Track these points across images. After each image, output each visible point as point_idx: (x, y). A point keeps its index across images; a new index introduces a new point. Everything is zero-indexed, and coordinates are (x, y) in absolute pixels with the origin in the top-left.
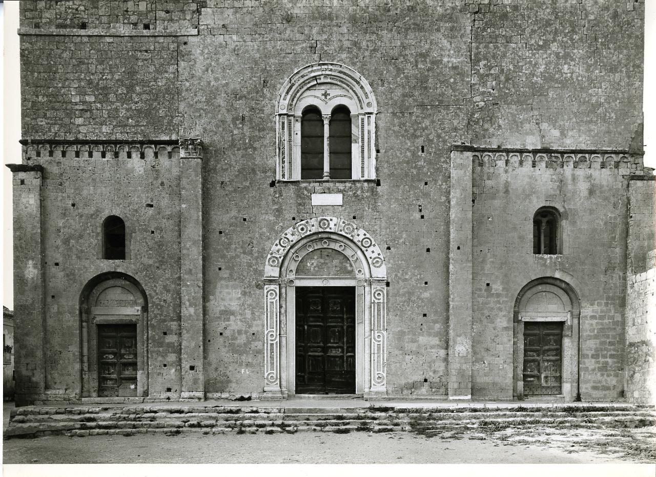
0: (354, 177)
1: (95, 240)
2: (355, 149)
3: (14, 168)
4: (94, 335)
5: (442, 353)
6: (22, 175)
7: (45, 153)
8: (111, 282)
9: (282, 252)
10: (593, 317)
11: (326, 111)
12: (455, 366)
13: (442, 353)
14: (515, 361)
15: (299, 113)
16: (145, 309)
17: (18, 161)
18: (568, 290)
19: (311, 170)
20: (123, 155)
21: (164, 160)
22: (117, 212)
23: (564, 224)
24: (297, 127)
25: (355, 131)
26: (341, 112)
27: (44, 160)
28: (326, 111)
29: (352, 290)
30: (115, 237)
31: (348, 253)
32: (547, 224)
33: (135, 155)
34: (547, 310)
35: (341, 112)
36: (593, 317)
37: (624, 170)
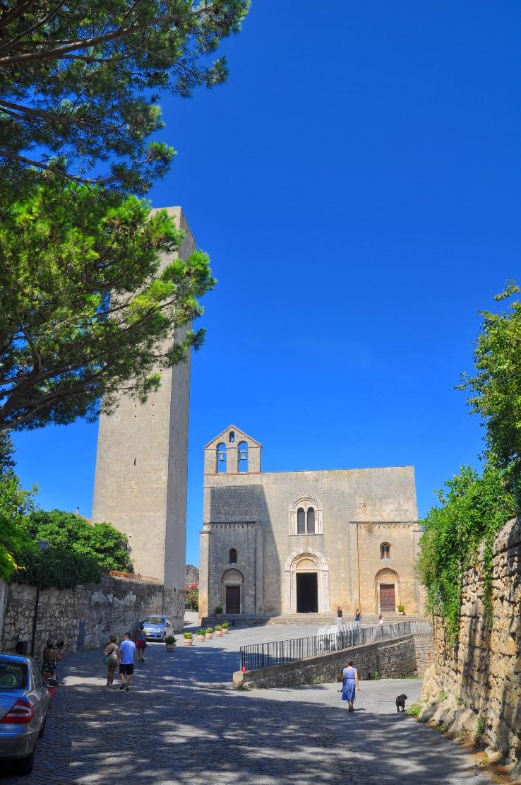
0: (316, 532)
1: (228, 558)
2: (316, 522)
4: (225, 591)
5: (349, 597)
8: (229, 572)
9: (291, 560)
10: (404, 582)
11: (306, 510)
12: (353, 602)
13: (349, 597)
16: (243, 582)
18: (394, 572)
19: (300, 528)
20: (236, 526)
21: (250, 528)
22: (235, 547)
23: (391, 548)
24: (296, 515)
25: (316, 516)
26: (311, 510)
28: (306, 510)
29: (316, 573)
30: (233, 555)
32: (385, 548)
33: (240, 527)
34: (387, 579)
35: (311, 510)
36: (404, 582)
37: (412, 528)
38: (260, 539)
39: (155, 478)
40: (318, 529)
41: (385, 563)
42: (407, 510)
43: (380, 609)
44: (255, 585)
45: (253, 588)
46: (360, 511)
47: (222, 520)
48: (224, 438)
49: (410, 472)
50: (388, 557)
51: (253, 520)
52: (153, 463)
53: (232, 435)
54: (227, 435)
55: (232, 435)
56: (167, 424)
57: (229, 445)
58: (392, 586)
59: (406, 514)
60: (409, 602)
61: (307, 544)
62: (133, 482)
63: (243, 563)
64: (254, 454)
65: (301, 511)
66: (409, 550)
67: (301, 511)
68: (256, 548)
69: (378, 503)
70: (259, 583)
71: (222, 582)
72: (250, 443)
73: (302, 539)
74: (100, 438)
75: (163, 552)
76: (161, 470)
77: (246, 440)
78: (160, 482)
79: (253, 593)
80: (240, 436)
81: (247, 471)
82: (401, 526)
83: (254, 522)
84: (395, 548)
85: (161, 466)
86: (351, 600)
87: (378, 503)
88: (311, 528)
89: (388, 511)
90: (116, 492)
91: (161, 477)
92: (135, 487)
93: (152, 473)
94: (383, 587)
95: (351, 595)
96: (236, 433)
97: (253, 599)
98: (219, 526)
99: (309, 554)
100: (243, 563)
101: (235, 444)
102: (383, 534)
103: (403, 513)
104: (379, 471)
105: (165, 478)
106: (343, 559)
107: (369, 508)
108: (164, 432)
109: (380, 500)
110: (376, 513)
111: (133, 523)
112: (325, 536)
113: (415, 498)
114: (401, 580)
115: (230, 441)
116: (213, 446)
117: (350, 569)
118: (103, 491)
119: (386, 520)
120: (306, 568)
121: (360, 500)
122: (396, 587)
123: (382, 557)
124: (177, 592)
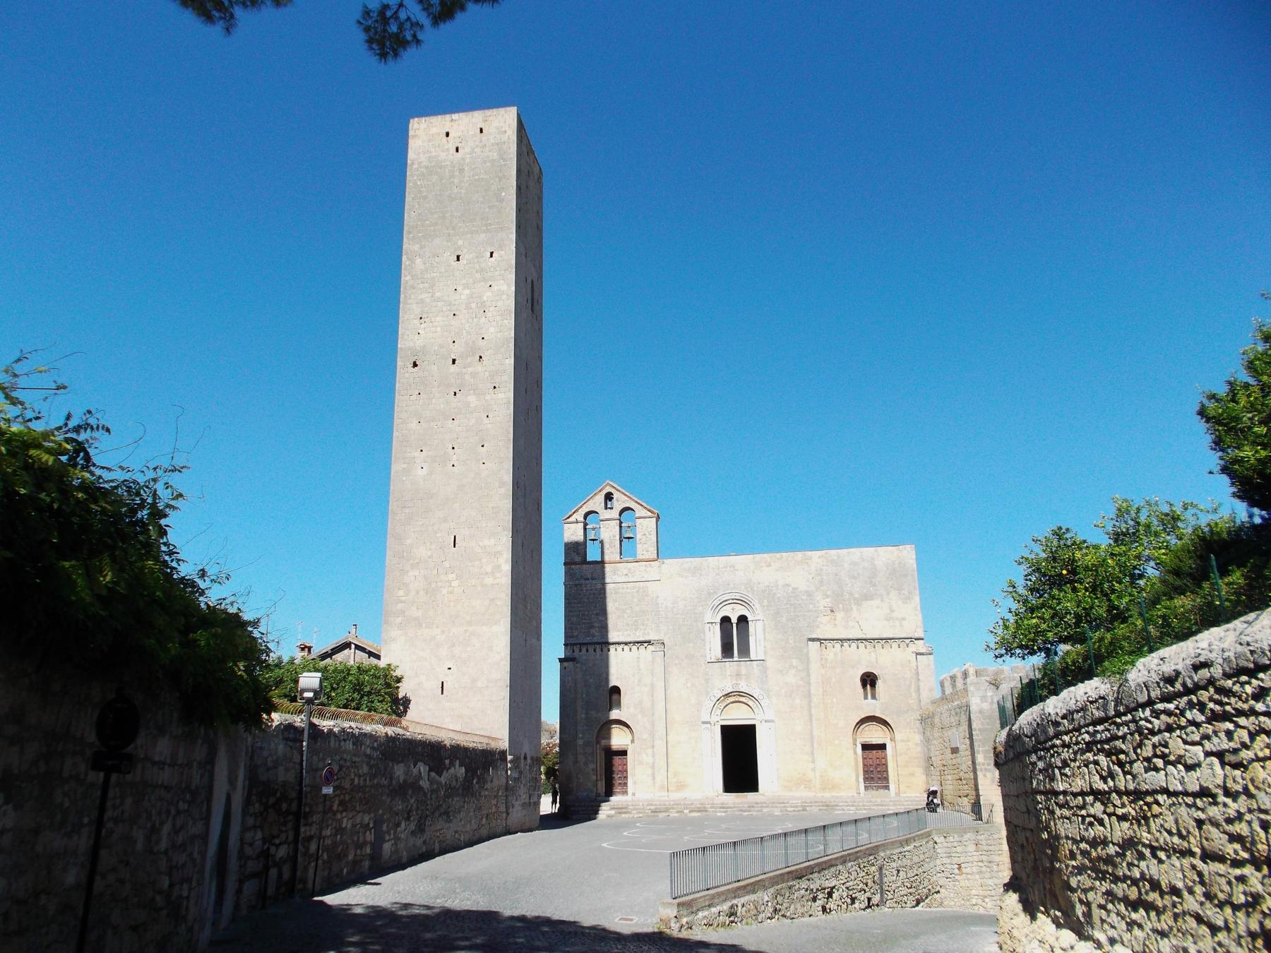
0: (753, 656)
3: (561, 660)
6: (566, 664)
7: (576, 649)
11: (734, 620)
14: (857, 770)
15: (718, 620)
16: (633, 741)
17: (563, 656)
18: (885, 723)
23: (879, 684)
24: (718, 627)
26: (743, 620)
27: (577, 654)
28: (734, 620)
31: (750, 703)
34: (874, 734)
35: (743, 620)
38: (659, 669)
39: (489, 569)
40: (756, 648)
41: (871, 707)
42: (904, 619)
43: (862, 785)
44: (653, 747)
45: (650, 751)
46: (824, 620)
47: (595, 640)
48: (597, 503)
49: (907, 554)
50: (874, 697)
51: (647, 638)
52: (486, 542)
53: (609, 497)
54: (600, 498)
55: (609, 497)
56: (508, 478)
57: (605, 514)
58: (882, 747)
59: (901, 625)
60: (912, 775)
61: (738, 675)
62: (451, 576)
63: (632, 710)
64: (645, 528)
65: (726, 620)
66: (910, 686)
67: (726, 620)
68: (652, 685)
69: (855, 608)
70: (657, 743)
71: (598, 742)
72: (640, 512)
73: (730, 666)
74: (393, 505)
75: (506, 693)
76: (500, 553)
77: (633, 505)
78: (498, 575)
79: (650, 760)
80: (620, 501)
81: (635, 556)
82: (895, 645)
83: (649, 642)
84: (885, 681)
85: (499, 548)
86: (814, 770)
87: (855, 608)
88: (745, 651)
89: (872, 620)
90: (422, 593)
91: (499, 566)
92: (455, 584)
93: (484, 560)
94: (866, 747)
95: (813, 762)
96: (616, 495)
97: (649, 771)
98: (591, 649)
99: (740, 694)
100: (632, 710)
101: (614, 514)
102: (867, 659)
103: (897, 623)
104: (855, 554)
105: (507, 567)
106: (798, 701)
107: (840, 615)
108: (503, 491)
109: (858, 602)
110: (851, 624)
111: (453, 645)
112: (769, 663)
113: (917, 599)
114: (898, 736)
115: (606, 508)
116: (579, 516)
117: (811, 716)
118: (401, 593)
119: (868, 636)
120: (738, 716)
121: (826, 602)
122: (888, 747)
123: (866, 698)
124: (529, 761)
